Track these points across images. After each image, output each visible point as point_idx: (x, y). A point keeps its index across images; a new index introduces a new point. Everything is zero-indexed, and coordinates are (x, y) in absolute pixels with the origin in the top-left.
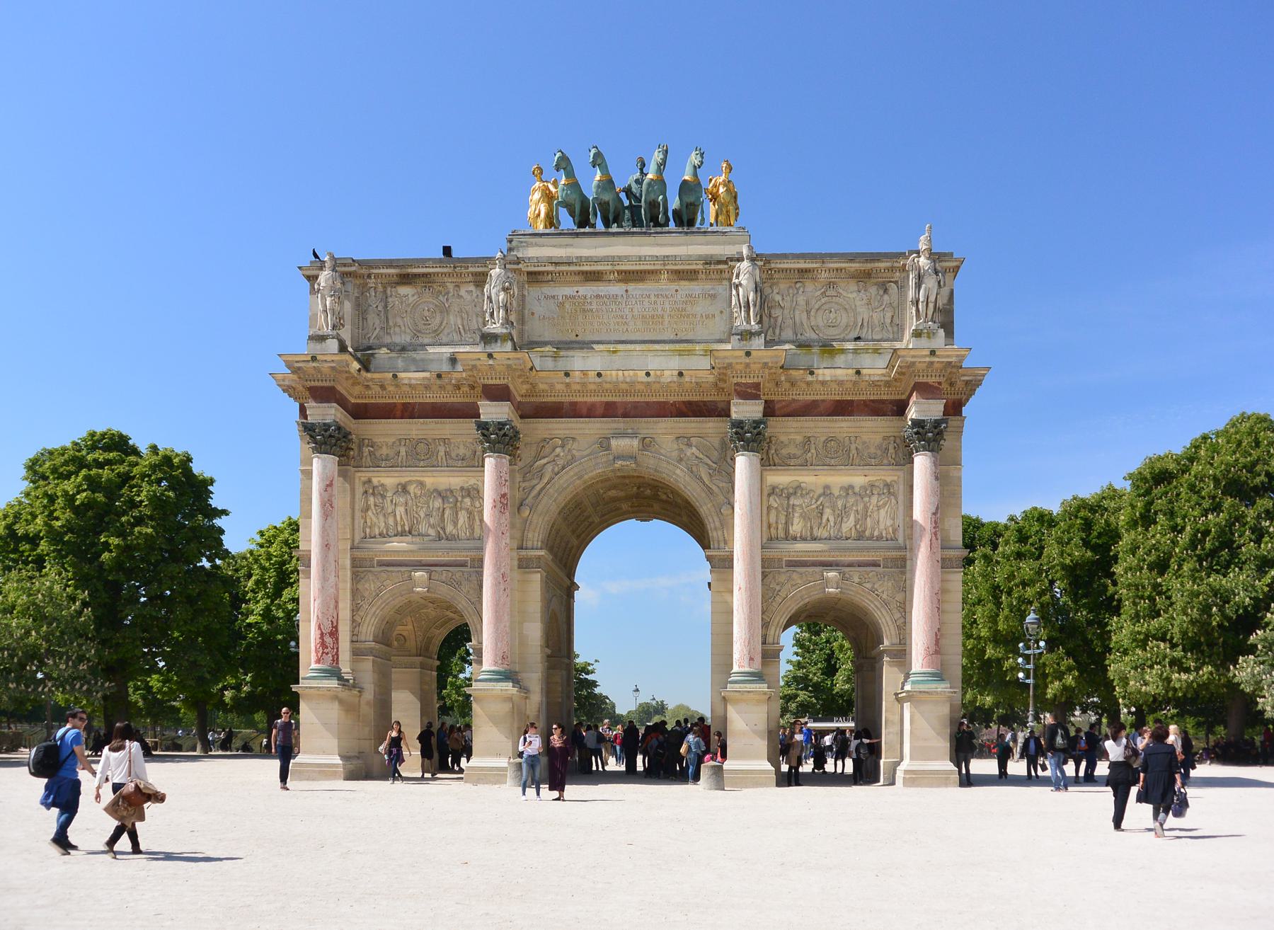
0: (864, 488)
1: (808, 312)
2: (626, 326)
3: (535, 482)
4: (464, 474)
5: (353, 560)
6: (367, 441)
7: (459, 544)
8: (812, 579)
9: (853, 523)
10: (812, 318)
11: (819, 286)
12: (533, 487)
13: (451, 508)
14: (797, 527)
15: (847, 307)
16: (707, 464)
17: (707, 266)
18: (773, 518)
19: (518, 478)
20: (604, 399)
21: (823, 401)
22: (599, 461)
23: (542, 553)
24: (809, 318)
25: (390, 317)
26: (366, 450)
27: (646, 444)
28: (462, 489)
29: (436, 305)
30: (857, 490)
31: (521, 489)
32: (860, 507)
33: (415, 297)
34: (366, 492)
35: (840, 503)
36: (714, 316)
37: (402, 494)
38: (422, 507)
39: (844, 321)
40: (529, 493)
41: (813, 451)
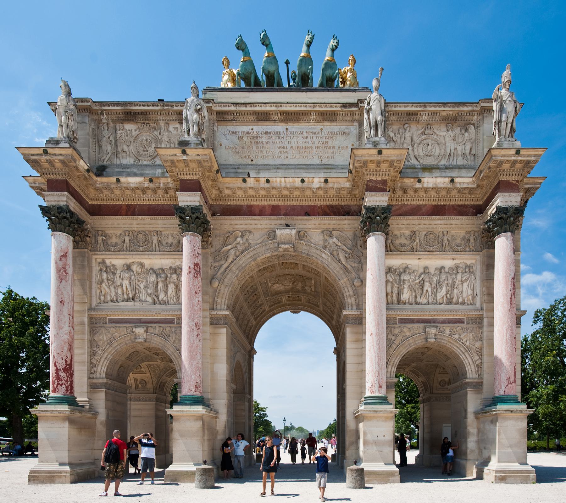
1: (413, 145)
2: (286, 154)
3: (222, 262)
4: (172, 257)
5: (91, 319)
7: (169, 307)
8: (417, 332)
9: (445, 293)
10: (415, 150)
11: (420, 128)
12: (221, 266)
13: (162, 281)
14: (406, 295)
15: (439, 142)
16: (344, 250)
18: (389, 290)
19: (211, 260)
22: (267, 247)
23: (227, 313)
24: (413, 150)
25: (119, 145)
27: (301, 235)
28: (171, 268)
29: (152, 138)
30: (447, 270)
31: (212, 268)
32: (450, 281)
33: (137, 131)
34: (101, 270)
35: (435, 279)
37: (127, 271)
39: (437, 152)
40: (218, 271)
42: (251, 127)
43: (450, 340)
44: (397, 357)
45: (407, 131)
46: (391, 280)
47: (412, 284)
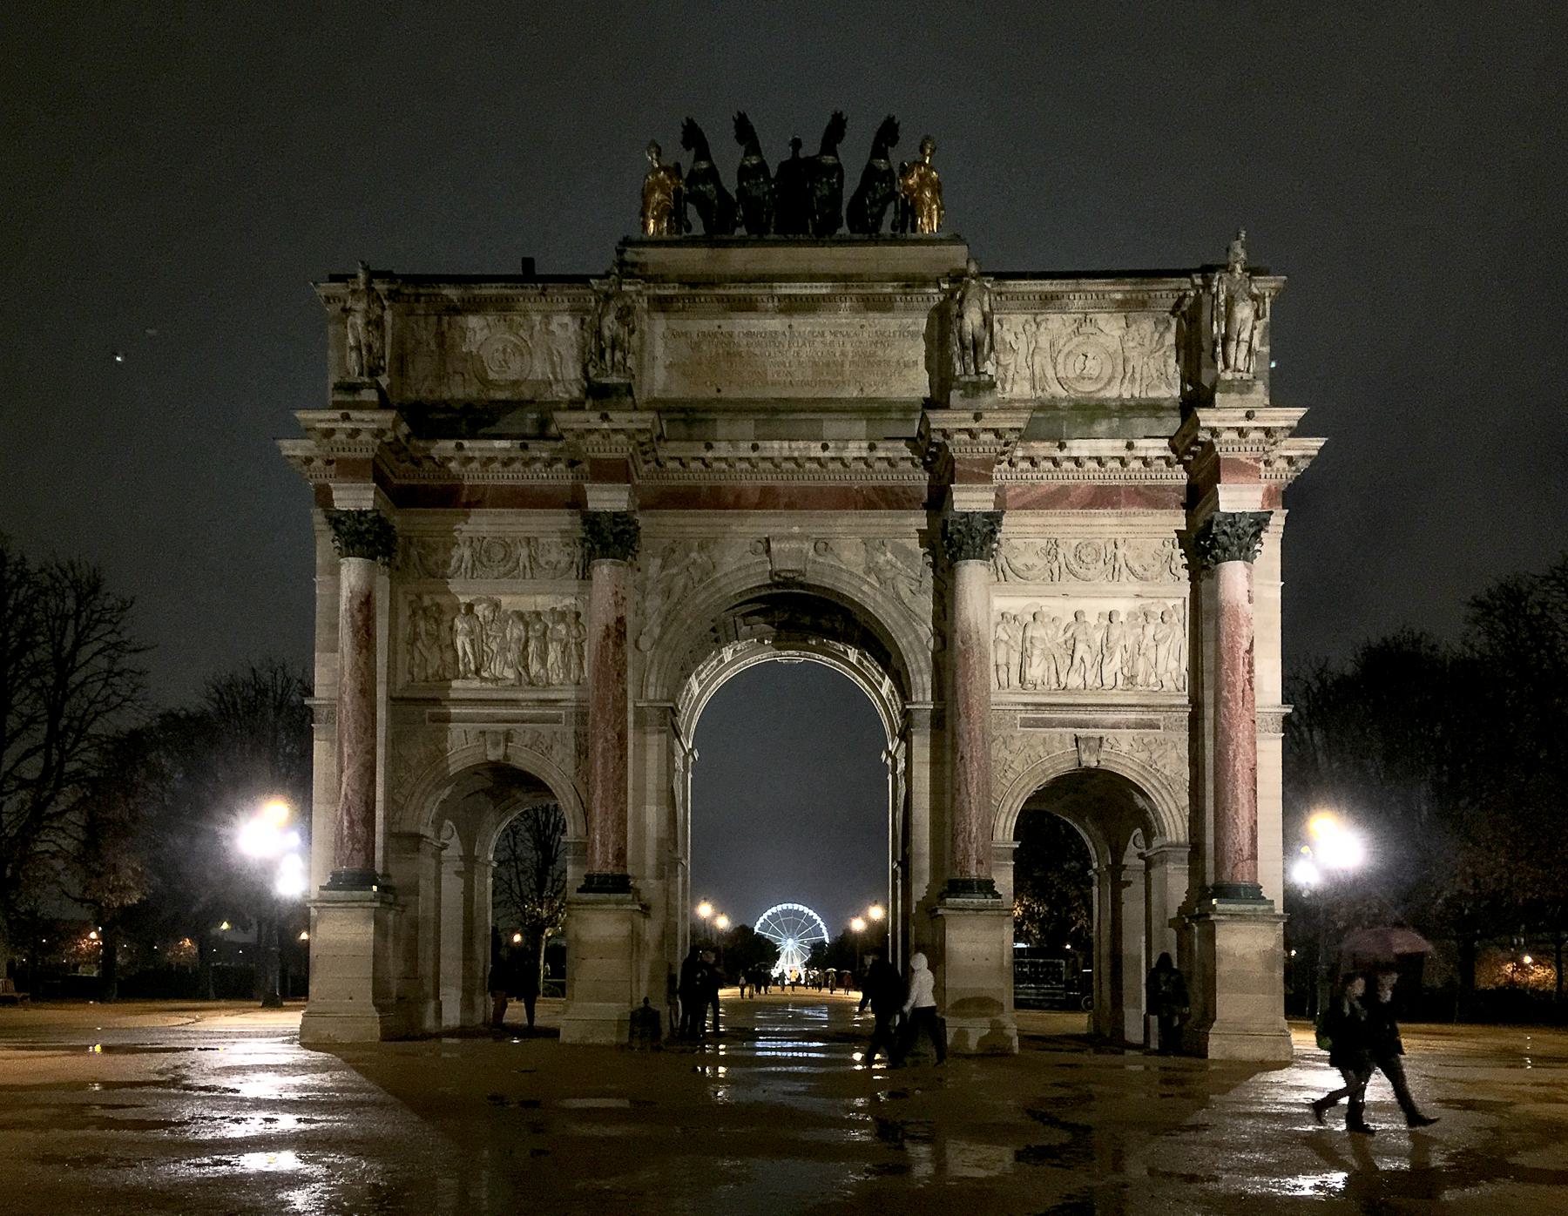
0: (1132, 615)
6: (415, 539)
9: (1119, 665)
13: (536, 638)
14: (1036, 671)
17: (908, 290)
18: (1001, 661)
20: (759, 483)
21: (1077, 487)
26: (414, 552)
27: (824, 545)
28: (553, 610)
30: (1123, 618)
31: (639, 612)
32: (1130, 642)
34: (414, 613)
35: (1098, 636)
36: (916, 363)
38: (495, 637)
41: (1061, 557)
42: (717, 322)
43: (1130, 764)
44: (1017, 797)
45: (1042, 329)
46: (1005, 637)
47: (1049, 645)
